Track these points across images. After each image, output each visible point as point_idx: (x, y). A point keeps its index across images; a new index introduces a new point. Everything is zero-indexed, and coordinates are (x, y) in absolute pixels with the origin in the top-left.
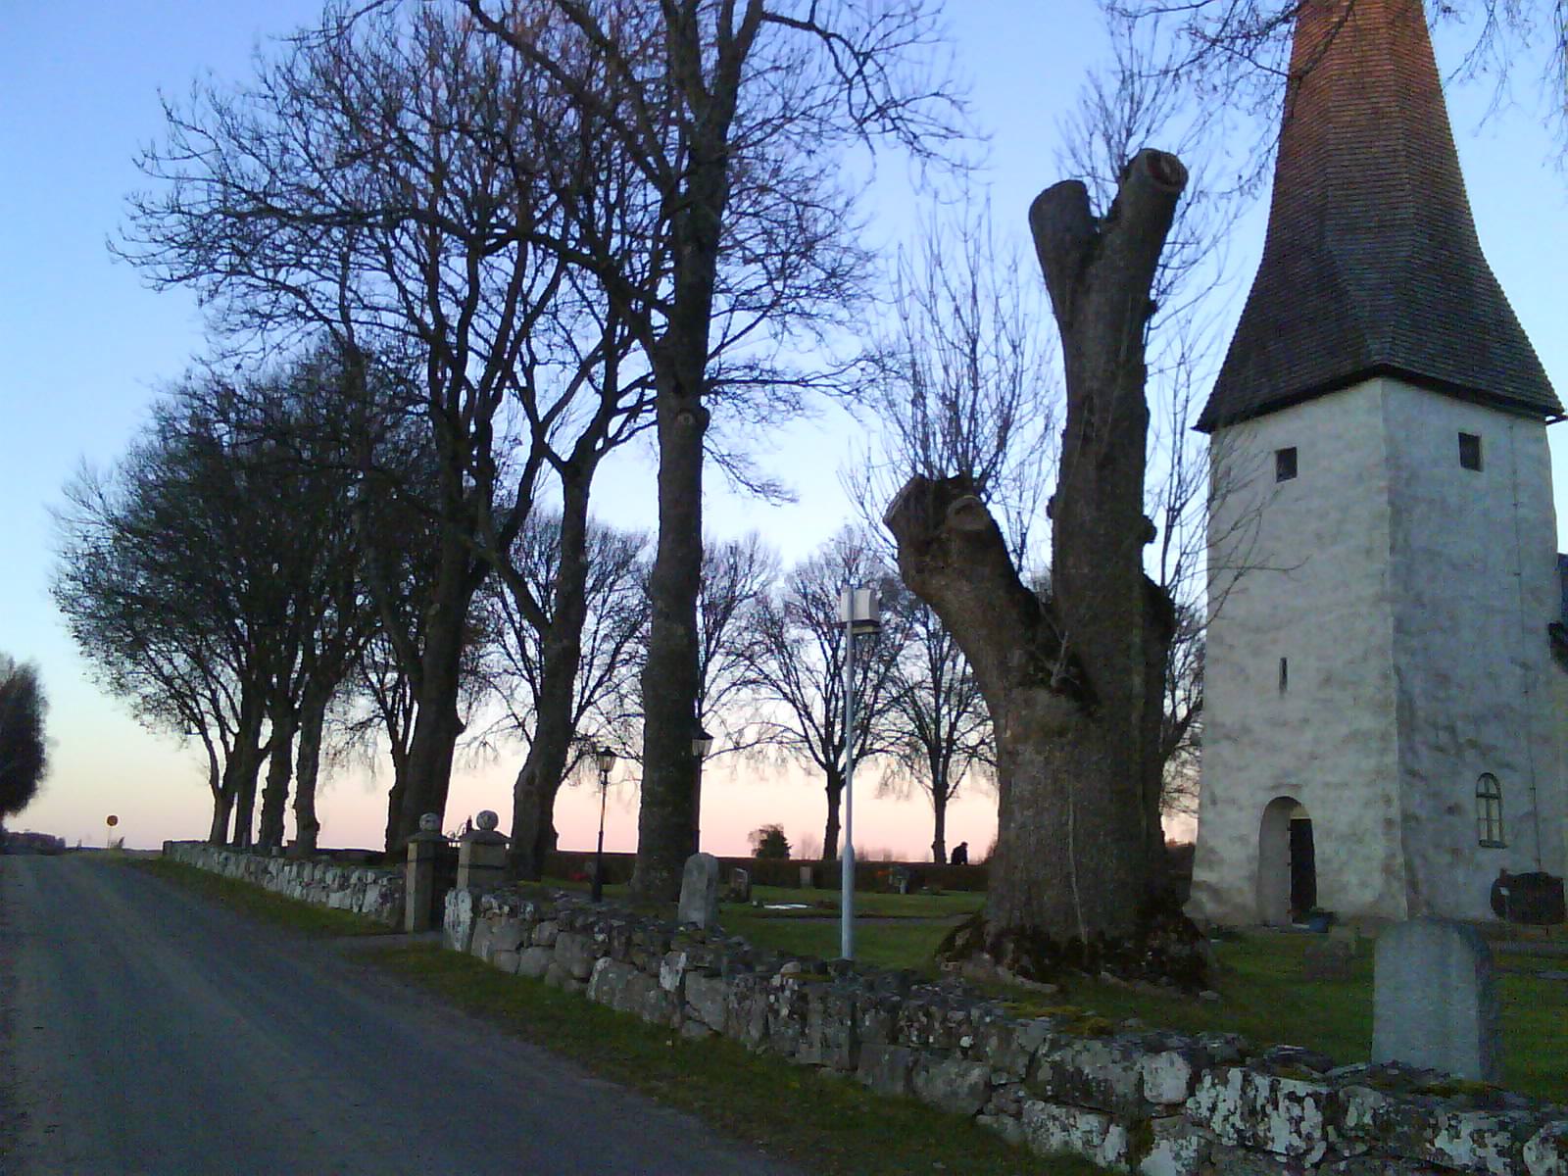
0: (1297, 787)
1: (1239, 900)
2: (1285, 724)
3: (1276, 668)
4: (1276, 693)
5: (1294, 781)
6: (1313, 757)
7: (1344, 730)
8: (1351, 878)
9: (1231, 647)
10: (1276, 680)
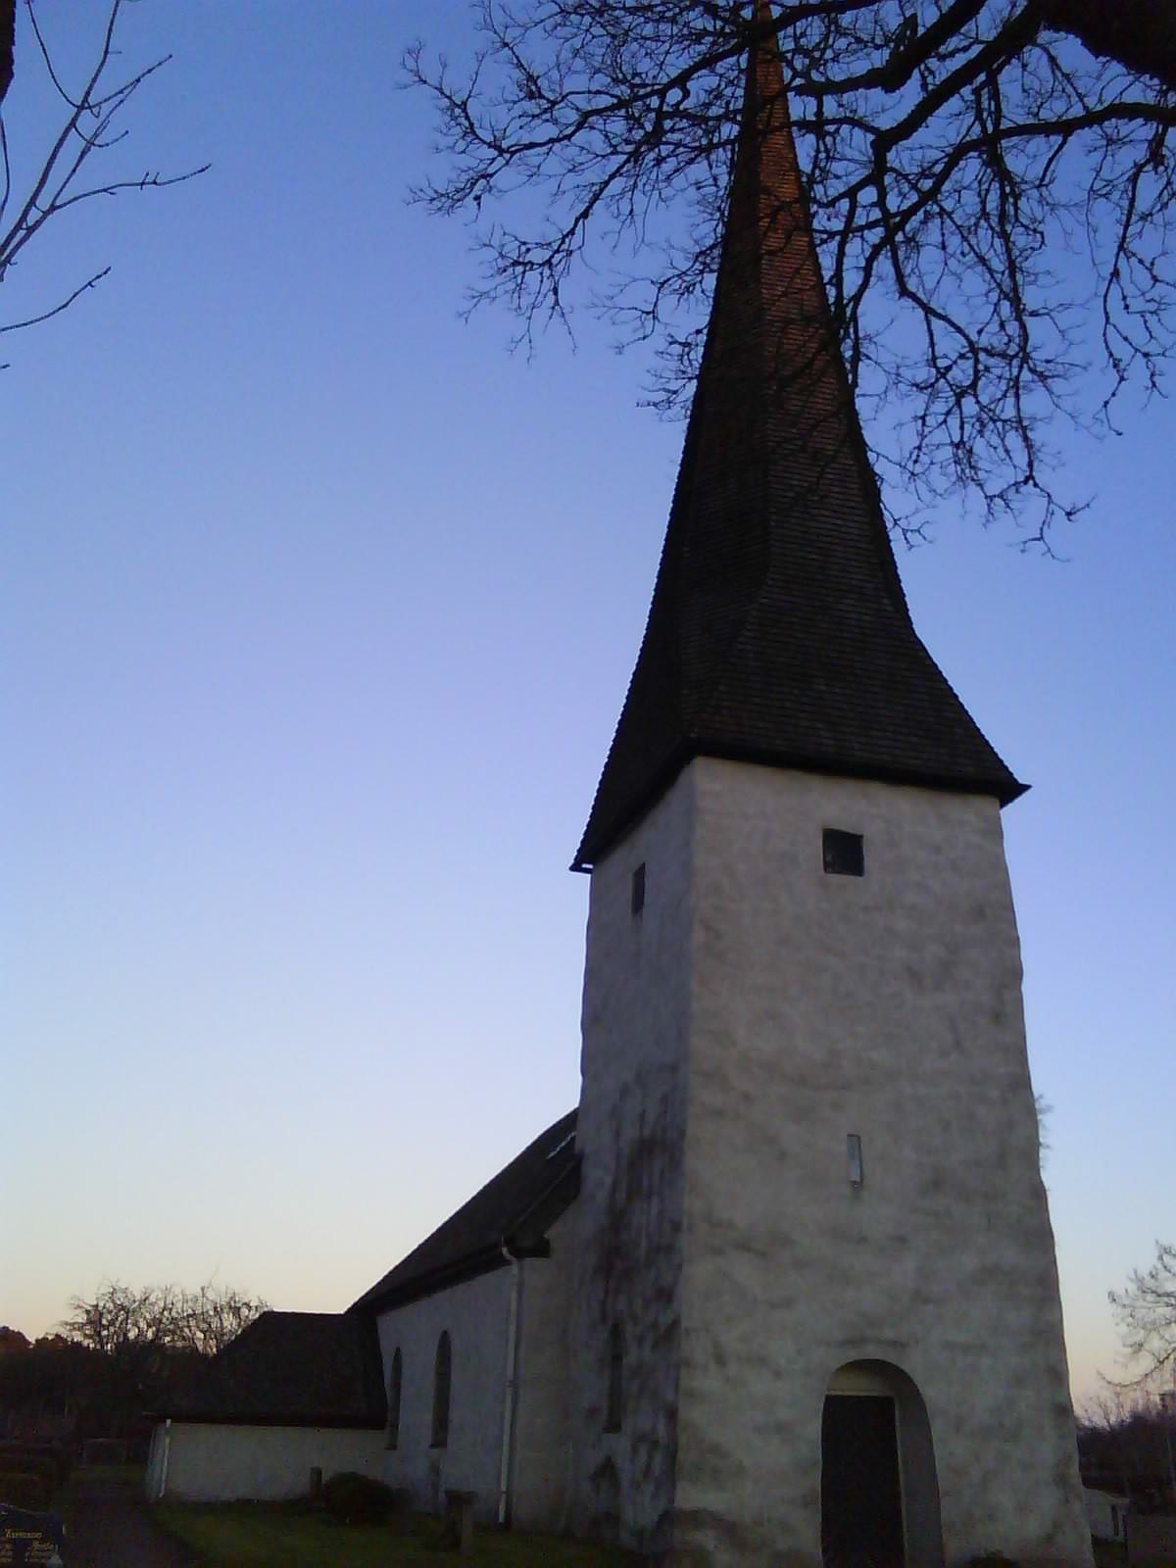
0: (897, 1345)
1: (783, 1544)
2: (863, 1240)
5: (888, 1333)
7: (969, 1262)
9: (746, 1097)
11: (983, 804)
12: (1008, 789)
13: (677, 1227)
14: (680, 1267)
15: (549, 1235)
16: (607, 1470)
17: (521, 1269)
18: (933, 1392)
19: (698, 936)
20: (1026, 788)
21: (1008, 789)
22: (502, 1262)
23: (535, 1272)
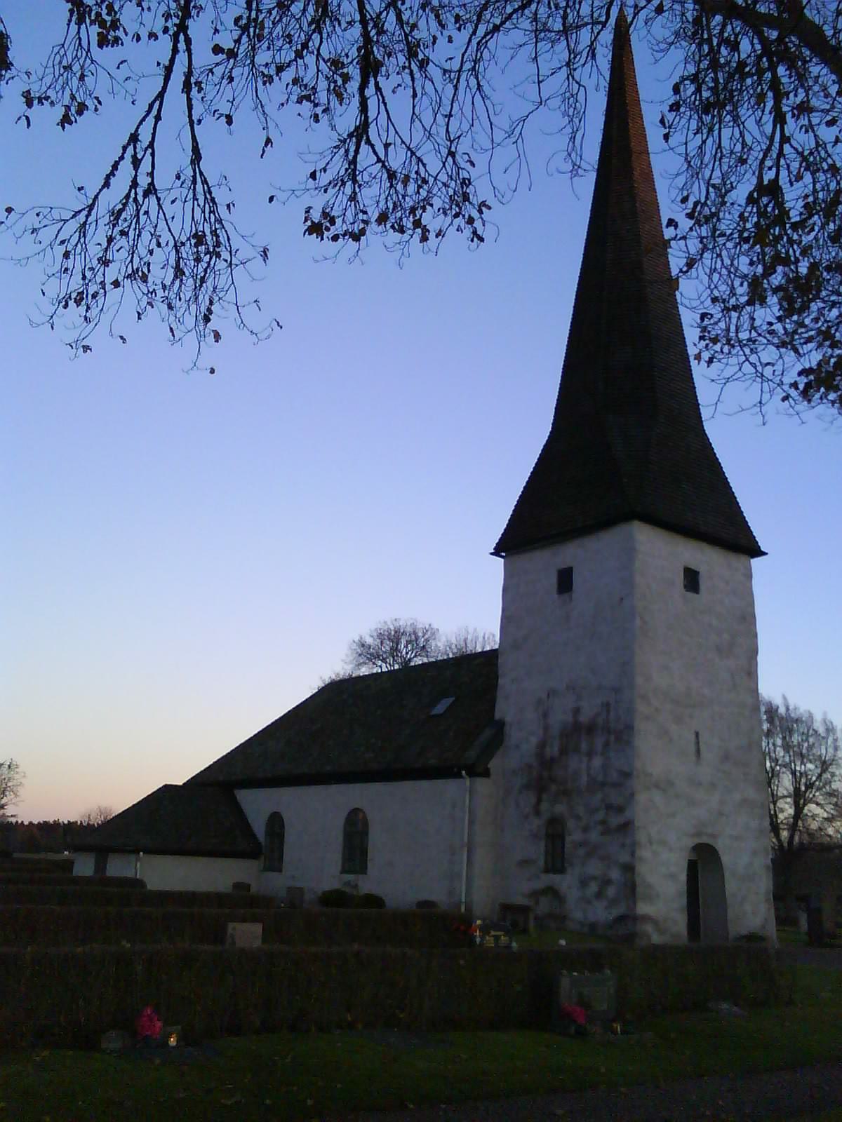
0: (714, 836)
2: (700, 784)
3: (693, 737)
4: (694, 758)
6: (721, 814)
7: (737, 796)
8: (748, 908)
9: (657, 710)
10: (693, 748)
11: (743, 558)
12: (756, 552)
13: (627, 775)
14: (632, 795)
15: (489, 766)
16: (552, 891)
17: (470, 781)
18: (726, 859)
19: (638, 622)
20: (764, 554)
21: (756, 552)
22: (461, 776)
23: (483, 786)
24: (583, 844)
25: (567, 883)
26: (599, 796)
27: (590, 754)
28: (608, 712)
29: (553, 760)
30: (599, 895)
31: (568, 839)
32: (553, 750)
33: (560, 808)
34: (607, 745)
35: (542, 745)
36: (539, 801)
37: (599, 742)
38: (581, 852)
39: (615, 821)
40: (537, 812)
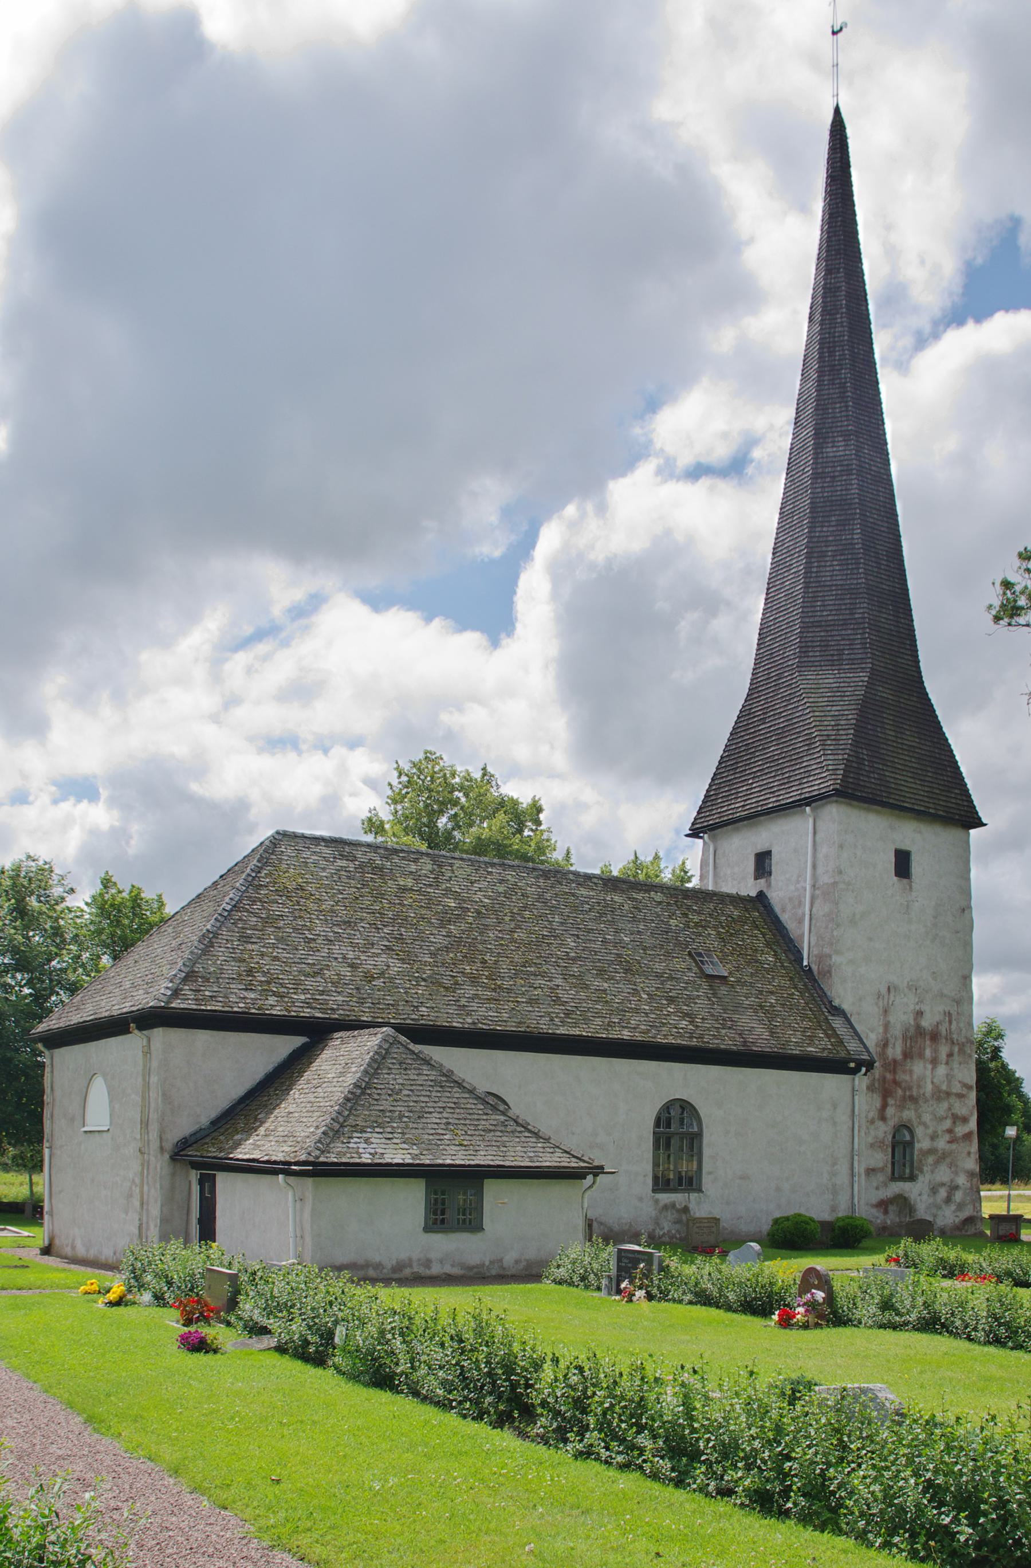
16: (902, 1202)
24: (931, 1151)
25: (917, 1191)
26: (945, 1105)
27: (935, 1062)
28: (950, 1022)
29: (895, 1061)
30: (948, 1200)
31: (917, 1146)
32: (895, 1051)
33: (908, 1114)
34: (950, 1055)
35: (885, 1044)
36: (884, 1106)
37: (944, 1050)
38: (931, 1160)
39: (961, 1130)
40: (883, 1118)
